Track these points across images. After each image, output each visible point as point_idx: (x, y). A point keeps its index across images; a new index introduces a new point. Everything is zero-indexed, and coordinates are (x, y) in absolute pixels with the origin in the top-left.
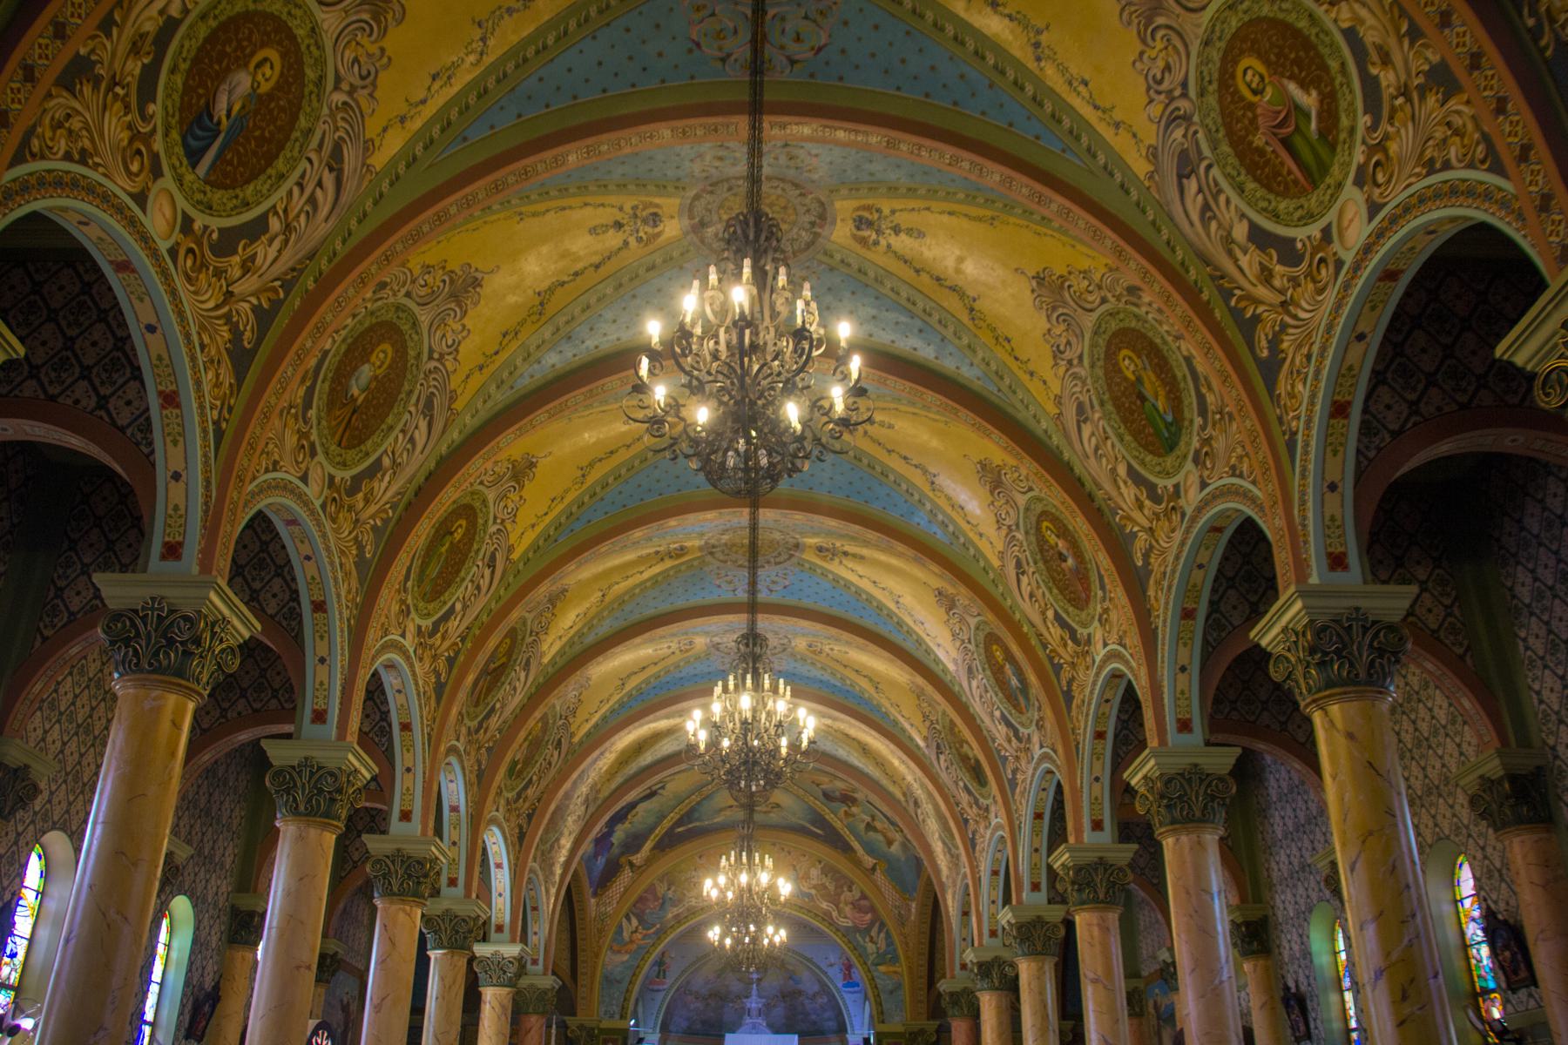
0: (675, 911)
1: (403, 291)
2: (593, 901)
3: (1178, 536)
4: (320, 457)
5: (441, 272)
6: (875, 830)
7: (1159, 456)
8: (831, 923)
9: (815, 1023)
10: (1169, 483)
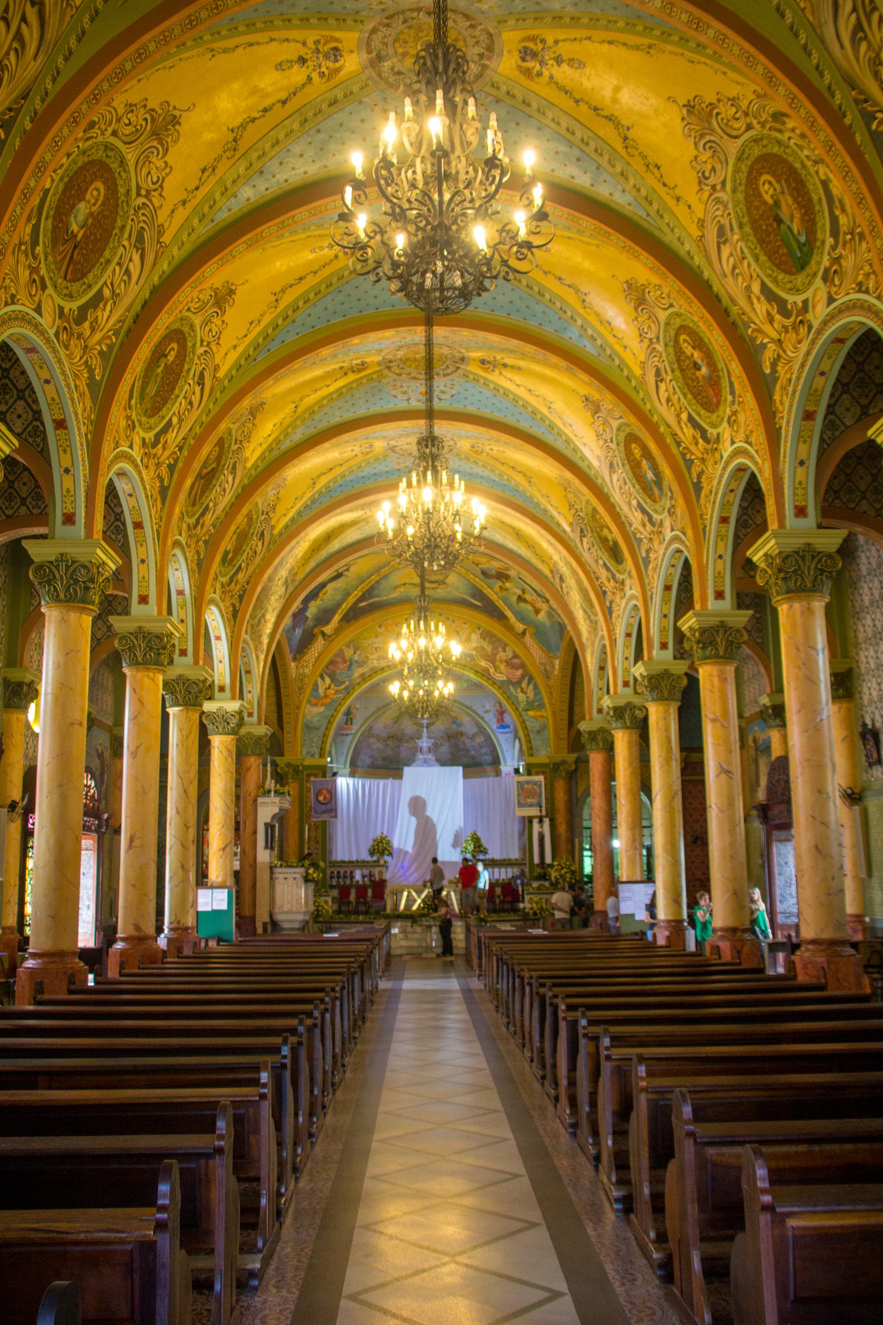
0: (361, 670)
1: (110, 130)
2: (293, 664)
3: (804, 347)
4: (50, 290)
5: (142, 110)
6: (525, 601)
7: (791, 274)
8: (489, 678)
9: (474, 757)
10: (799, 299)
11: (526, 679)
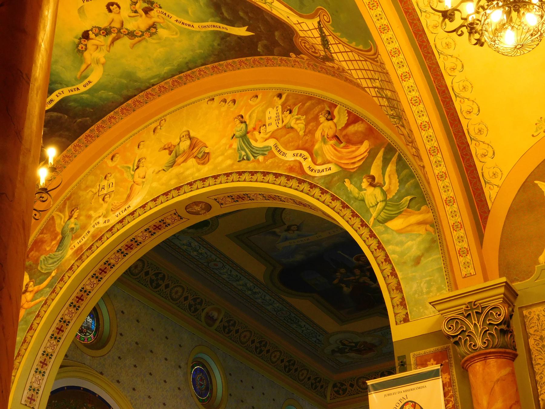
11: (381, 154)
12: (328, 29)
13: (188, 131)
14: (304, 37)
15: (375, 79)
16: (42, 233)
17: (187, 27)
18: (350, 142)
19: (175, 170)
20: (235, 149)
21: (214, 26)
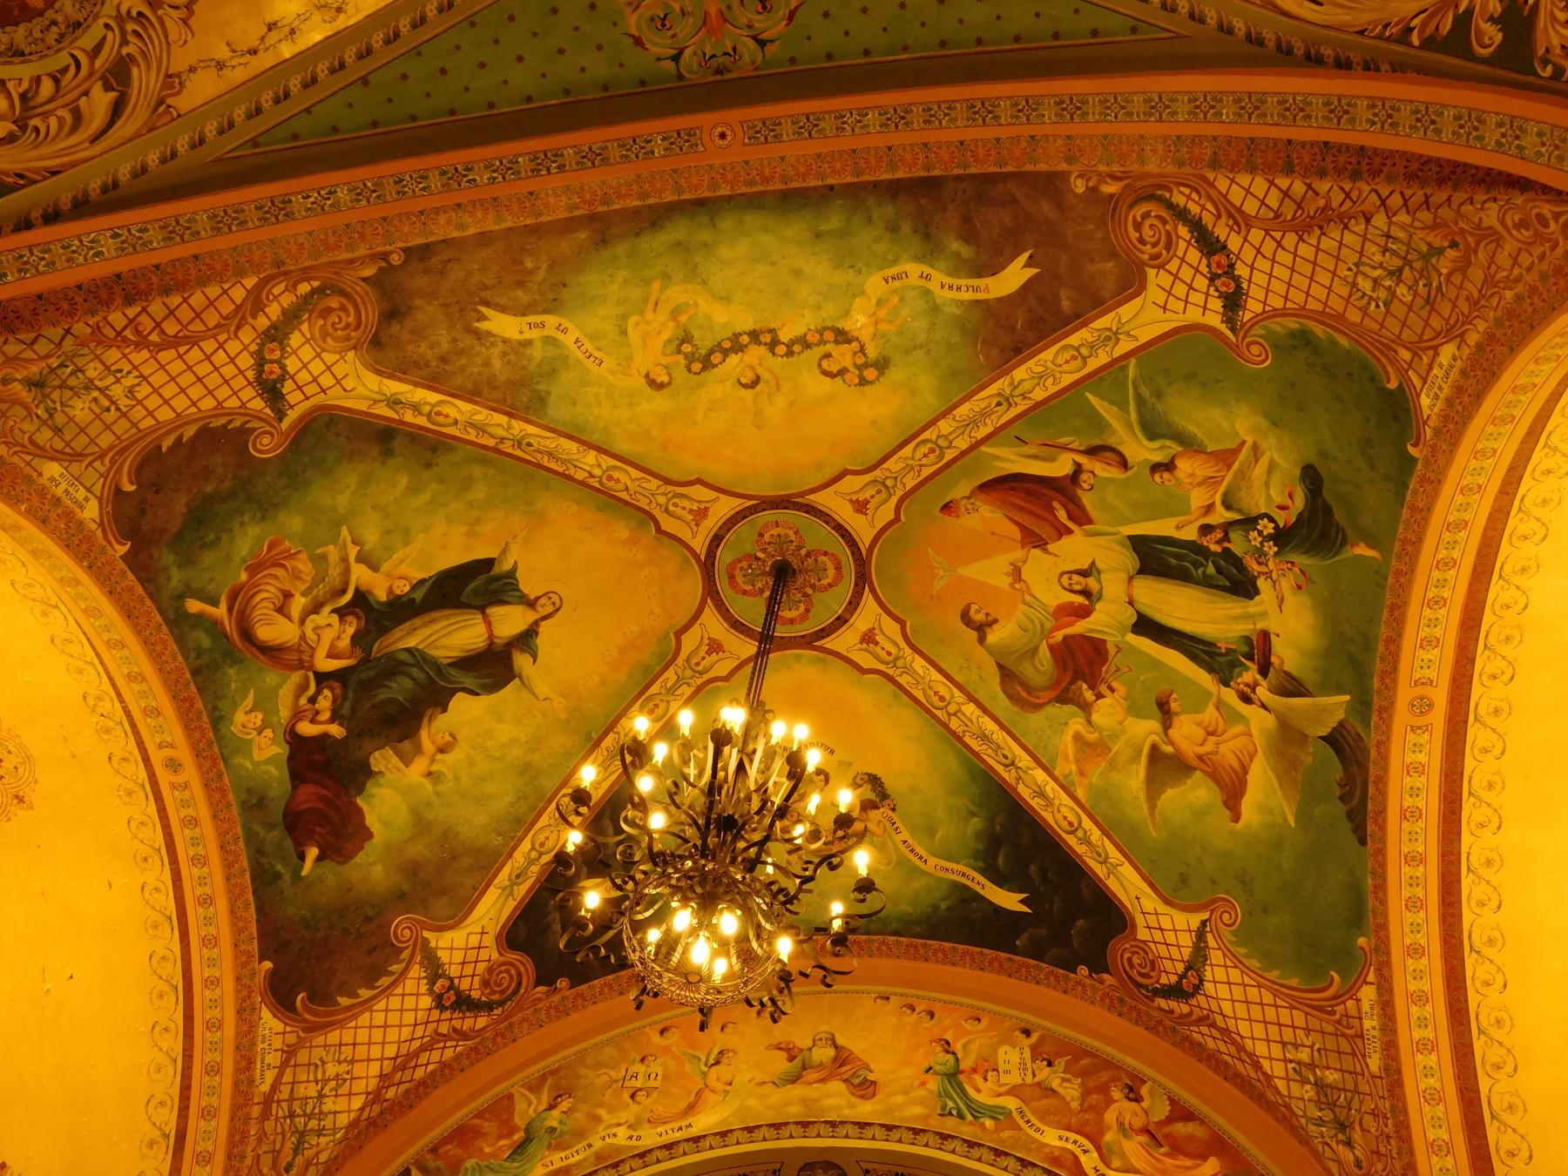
12: (1218, 937)
13: (833, 1035)
14: (1144, 942)
15: (1296, 1046)
16: (479, 1115)
17: (915, 860)
18: (1178, 1148)
19: (798, 1091)
20: (931, 1092)
21: (964, 875)
